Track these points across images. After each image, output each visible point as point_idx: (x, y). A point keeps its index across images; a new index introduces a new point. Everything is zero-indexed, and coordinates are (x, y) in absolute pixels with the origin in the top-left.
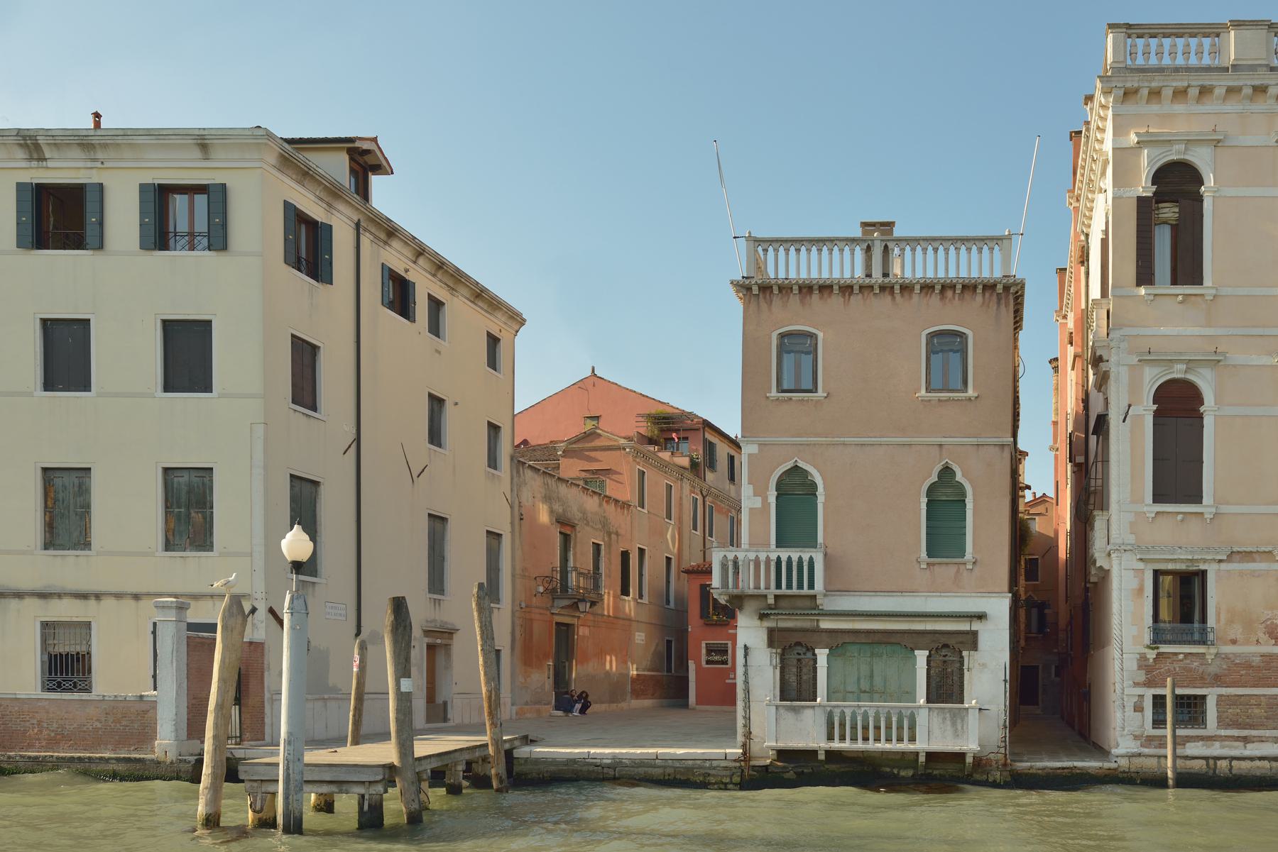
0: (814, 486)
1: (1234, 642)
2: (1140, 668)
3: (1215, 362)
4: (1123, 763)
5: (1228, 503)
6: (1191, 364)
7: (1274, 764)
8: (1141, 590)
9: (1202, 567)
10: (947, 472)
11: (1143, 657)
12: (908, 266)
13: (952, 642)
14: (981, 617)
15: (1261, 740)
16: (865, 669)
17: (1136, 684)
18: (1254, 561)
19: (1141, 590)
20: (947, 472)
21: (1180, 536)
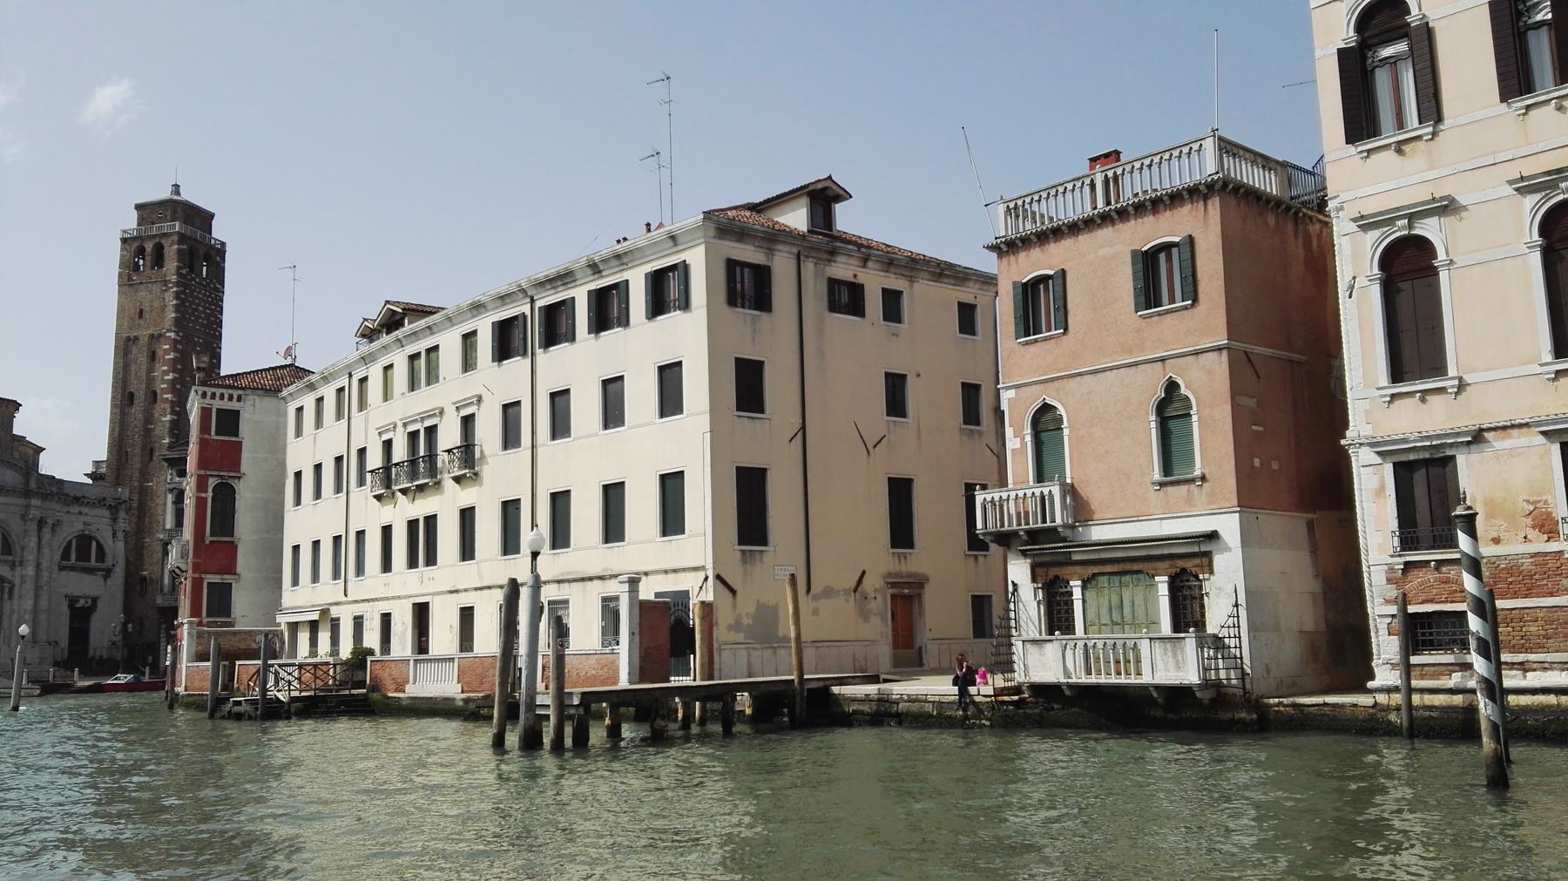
0: (1061, 419)
1: (1496, 541)
2: (1389, 581)
3: (1446, 207)
4: (1382, 698)
5: (1473, 371)
6: (1412, 218)
7: (1564, 699)
8: (1382, 488)
9: (1449, 453)
10: (1172, 387)
11: (1391, 569)
12: (1134, 187)
13: (1189, 564)
14: (1213, 536)
15: (1545, 667)
16: (1115, 599)
17: (1387, 602)
18: (1511, 437)
19: (1382, 488)
20: (1172, 387)
21: (1420, 418)
